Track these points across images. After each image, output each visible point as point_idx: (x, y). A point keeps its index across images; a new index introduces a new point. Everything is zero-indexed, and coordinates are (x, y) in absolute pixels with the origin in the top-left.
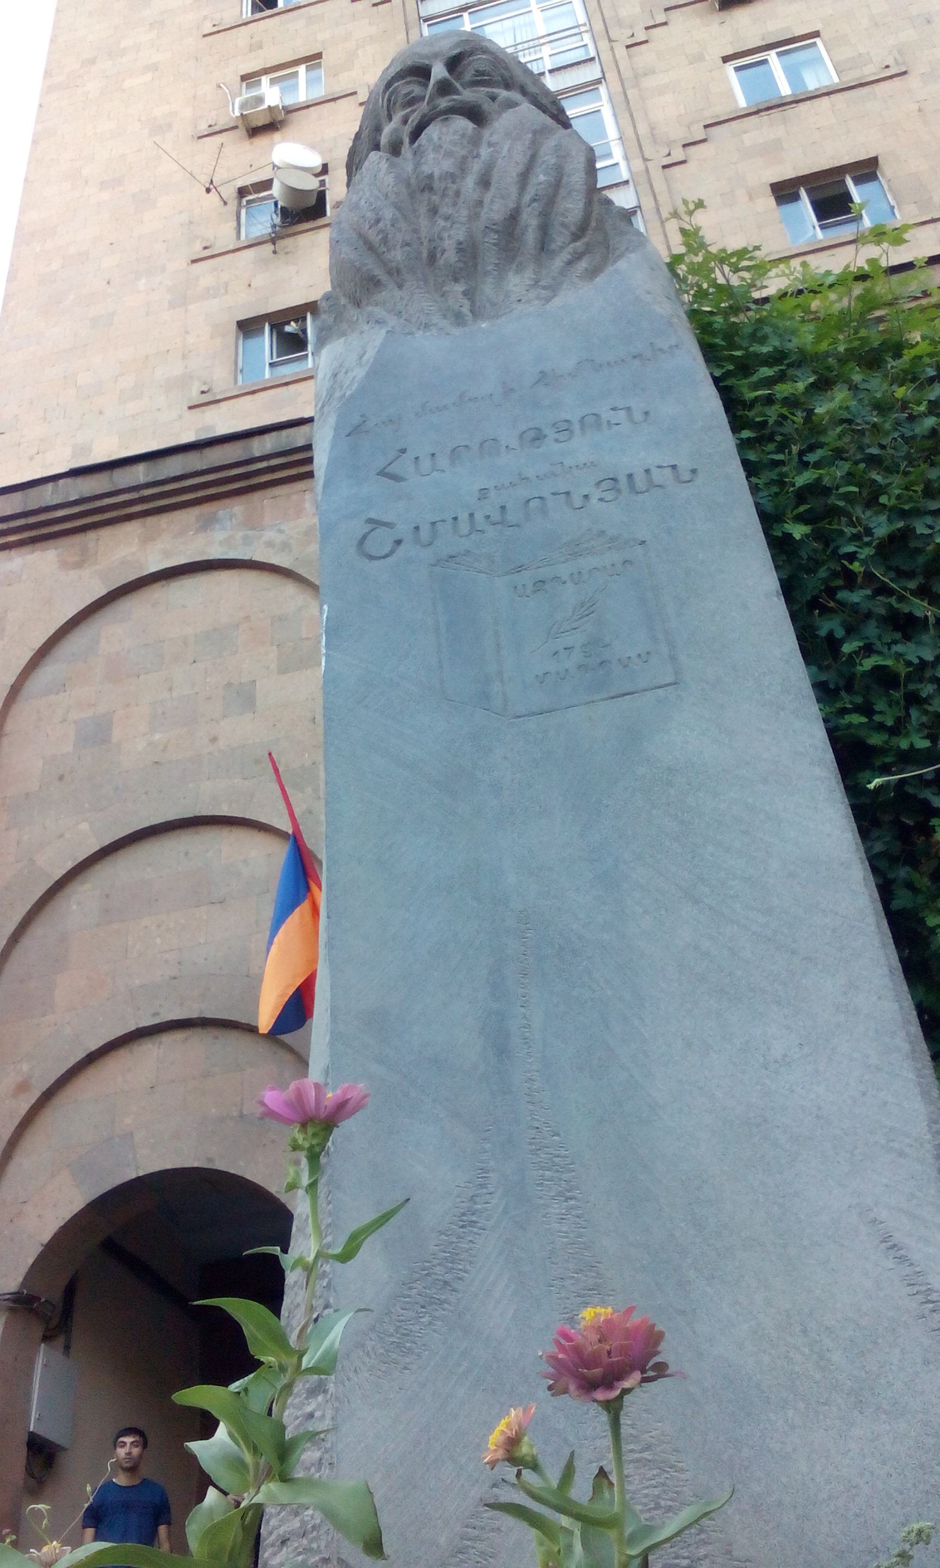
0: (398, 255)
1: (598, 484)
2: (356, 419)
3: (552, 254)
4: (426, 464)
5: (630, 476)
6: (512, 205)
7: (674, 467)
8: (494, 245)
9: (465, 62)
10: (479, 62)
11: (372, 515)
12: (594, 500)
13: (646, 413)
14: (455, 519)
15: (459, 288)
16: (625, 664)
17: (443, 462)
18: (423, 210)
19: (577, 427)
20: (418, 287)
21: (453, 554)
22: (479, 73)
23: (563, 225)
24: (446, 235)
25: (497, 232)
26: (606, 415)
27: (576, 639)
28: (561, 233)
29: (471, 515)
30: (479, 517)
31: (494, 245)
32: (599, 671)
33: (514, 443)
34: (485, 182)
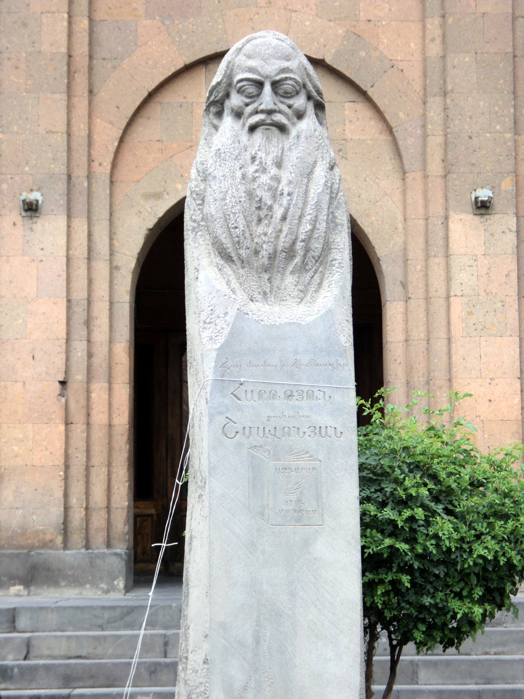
0: (243, 252)
1: (309, 427)
2: (224, 360)
3: (307, 271)
4: (249, 395)
5: (320, 427)
6: (294, 238)
7: (335, 428)
8: (284, 258)
9: (281, 83)
10: (288, 86)
11: (228, 416)
12: (307, 436)
13: (330, 397)
14: (258, 428)
15: (266, 276)
16: (308, 512)
17: (256, 396)
18: (255, 219)
19: (305, 395)
20: (250, 273)
21: (257, 445)
22: (286, 93)
23: (313, 257)
24: (265, 246)
25: (286, 252)
26: (317, 393)
27: (294, 498)
28: (312, 261)
29: (264, 428)
30: (267, 430)
31: (284, 258)
32: (299, 516)
33: (282, 396)
34: (284, 218)
